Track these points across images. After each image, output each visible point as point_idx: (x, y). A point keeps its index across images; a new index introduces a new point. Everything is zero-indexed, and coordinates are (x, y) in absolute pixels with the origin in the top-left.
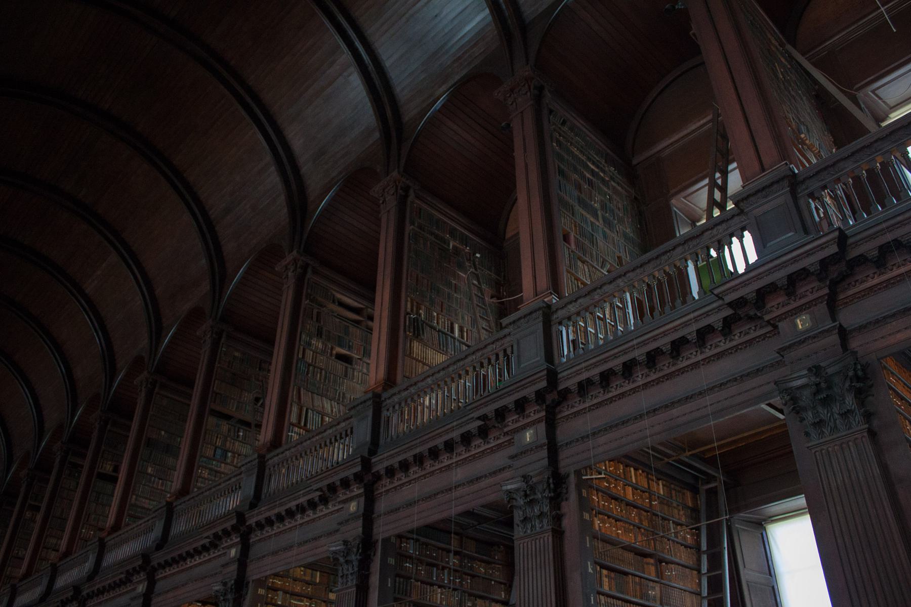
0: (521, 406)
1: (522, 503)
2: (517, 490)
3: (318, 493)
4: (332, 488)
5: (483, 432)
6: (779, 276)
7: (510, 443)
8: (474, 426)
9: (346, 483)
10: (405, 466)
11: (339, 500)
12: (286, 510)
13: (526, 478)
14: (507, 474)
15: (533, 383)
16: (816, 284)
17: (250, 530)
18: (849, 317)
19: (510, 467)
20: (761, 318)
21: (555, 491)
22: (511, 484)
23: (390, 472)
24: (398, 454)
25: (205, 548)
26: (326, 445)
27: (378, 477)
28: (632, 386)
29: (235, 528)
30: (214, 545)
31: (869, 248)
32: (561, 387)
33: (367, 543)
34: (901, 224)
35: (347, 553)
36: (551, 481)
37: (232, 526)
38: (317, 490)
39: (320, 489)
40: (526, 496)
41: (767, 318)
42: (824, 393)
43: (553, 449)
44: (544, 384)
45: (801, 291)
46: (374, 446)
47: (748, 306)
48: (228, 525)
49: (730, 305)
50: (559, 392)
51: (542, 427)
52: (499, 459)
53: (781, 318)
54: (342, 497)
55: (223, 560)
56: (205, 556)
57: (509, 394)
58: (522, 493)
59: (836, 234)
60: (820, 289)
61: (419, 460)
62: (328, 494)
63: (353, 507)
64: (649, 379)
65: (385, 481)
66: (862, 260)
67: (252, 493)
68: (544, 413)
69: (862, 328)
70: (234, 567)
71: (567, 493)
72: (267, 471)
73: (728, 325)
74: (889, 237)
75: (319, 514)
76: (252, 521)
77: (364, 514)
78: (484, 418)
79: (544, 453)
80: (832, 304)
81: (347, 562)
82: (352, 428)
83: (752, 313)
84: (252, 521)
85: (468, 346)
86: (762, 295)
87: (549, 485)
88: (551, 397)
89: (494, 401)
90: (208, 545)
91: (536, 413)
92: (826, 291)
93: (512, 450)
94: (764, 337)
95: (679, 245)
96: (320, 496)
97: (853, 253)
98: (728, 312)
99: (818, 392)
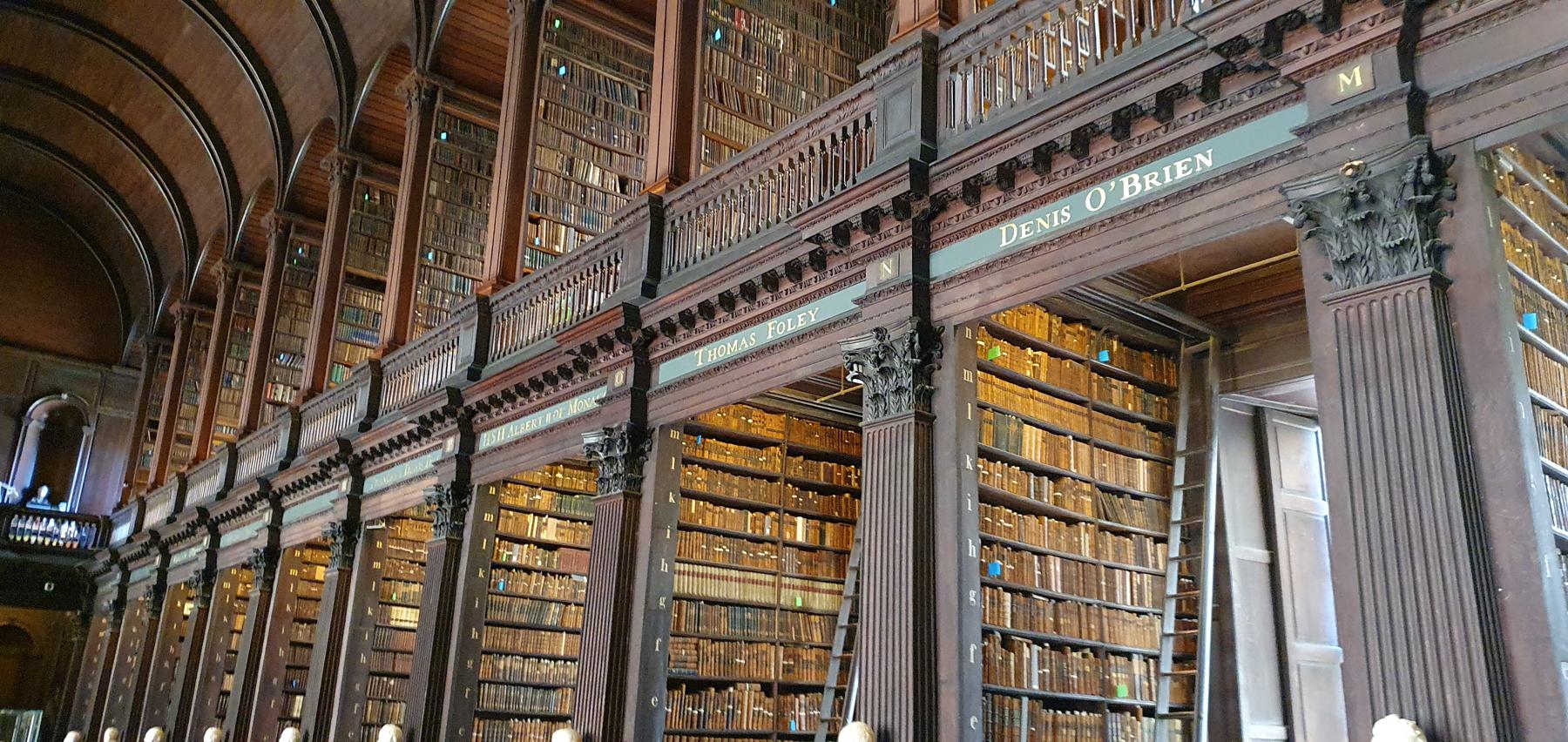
0: (872, 220)
2: (867, 351)
8: (803, 252)
13: (880, 332)
22: (859, 340)
43: (922, 288)
50: (933, 198)
51: (907, 254)
68: (910, 232)
78: (817, 239)
79: (908, 296)
91: (896, 230)
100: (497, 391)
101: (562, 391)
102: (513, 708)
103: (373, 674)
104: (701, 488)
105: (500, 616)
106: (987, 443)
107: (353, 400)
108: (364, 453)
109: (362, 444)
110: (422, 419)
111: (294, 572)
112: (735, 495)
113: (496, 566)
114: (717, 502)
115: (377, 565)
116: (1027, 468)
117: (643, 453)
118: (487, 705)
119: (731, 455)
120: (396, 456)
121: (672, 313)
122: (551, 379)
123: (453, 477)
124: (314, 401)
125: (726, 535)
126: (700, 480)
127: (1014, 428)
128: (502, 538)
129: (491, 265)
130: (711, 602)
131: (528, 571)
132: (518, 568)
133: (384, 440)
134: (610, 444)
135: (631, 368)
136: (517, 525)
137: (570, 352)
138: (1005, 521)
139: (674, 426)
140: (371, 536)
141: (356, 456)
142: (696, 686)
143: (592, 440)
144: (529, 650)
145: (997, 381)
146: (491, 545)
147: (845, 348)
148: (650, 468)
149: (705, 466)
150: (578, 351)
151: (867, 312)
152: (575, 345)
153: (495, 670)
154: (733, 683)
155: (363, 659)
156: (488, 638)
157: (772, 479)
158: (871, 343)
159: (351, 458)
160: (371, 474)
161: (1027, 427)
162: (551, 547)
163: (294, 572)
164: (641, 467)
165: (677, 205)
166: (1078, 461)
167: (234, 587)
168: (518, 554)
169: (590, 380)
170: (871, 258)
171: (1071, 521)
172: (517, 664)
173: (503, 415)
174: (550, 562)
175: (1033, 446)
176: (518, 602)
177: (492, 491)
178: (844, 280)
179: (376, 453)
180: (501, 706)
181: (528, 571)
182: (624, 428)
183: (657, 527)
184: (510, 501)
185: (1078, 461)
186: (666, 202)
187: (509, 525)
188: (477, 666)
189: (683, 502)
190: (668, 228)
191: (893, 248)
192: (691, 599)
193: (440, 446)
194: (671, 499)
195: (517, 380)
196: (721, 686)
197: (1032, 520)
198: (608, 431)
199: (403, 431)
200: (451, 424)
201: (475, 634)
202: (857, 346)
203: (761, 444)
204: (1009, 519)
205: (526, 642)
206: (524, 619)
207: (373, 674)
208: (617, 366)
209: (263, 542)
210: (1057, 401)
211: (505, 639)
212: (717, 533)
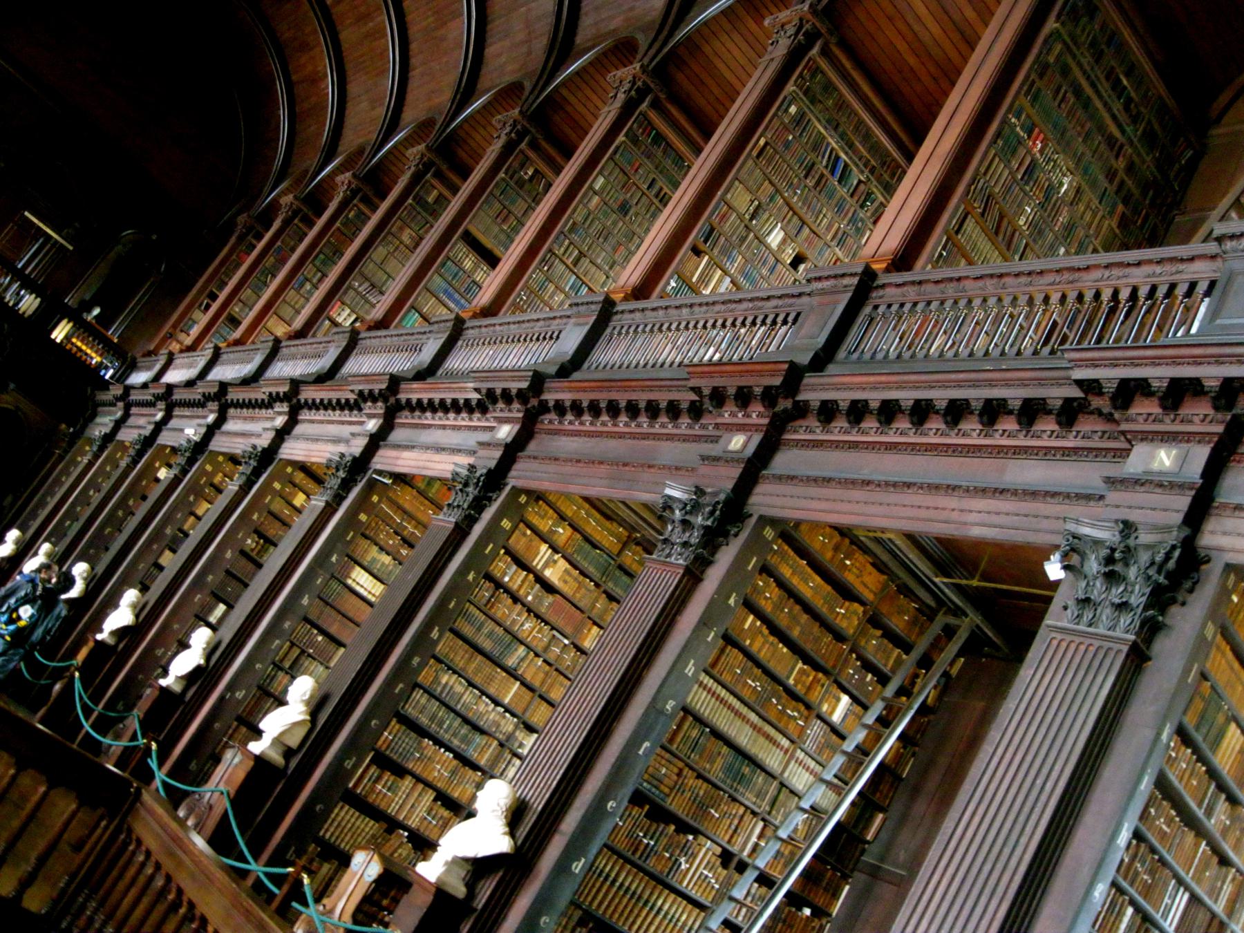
0: (1178, 393)
1: (1095, 571)
2: (1097, 543)
3: (694, 397)
4: (718, 397)
5: (1069, 414)
7: (1124, 453)
8: (1057, 394)
9: (744, 398)
10: (857, 412)
11: (719, 420)
12: (629, 402)
13: (1128, 528)
14: (1096, 509)
17: (544, 408)
19: (1102, 497)
22: (1093, 526)
23: (828, 412)
24: (887, 386)
25: (469, 407)
26: (724, 326)
27: (801, 411)
29: (522, 396)
30: (482, 407)
33: (733, 510)
35: (694, 507)
36: (1177, 553)
37: (520, 390)
38: (692, 389)
39: (696, 390)
40: (1110, 560)
46: (823, 359)
48: (515, 386)
51: (1201, 454)
52: (1088, 475)
54: (726, 417)
55: (485, 437)
56: (463, 420)
57: (1218, 360)
58: (1104, 552)
61: (921, 412)
62: (707, 404)
63: (737, 442)
65: (812, 421)
67: (571, 352)
68: (1220, 429)
70: (498, 454)
71: (1191, 591)
72: (608, 330)
75: (657, 429)
76: (550, 397)
77: (749, 461)
79: (1183, 502)
81: (686, 524)
82: (798, 314)
84: (550, 397)
87: (1168, 556)
89: (1175, 361)
90: (474, 403)
93: (1112, 470)
96: (693, 402)
100: (585, 399)
101: (657, 429)
102: (434, 728)
103: (306, 620)
104: (767, 607)
105: (467, 630)
106: (1190, 722)
107: (417, 349)
108: (409, 401)
109: (412, 391)
111: (277, 486)
112: (795, 633)
113: (489, 577)
114: (775, 630)
115: (363, 517)
116: (1212, 773)
117: (726, 535)
118: (410, 710)
119: (811, 586)
120: (438, 419)
121: (844, 397)
122: (653, 410)
123: (492, 464)
124: (379, 333)
125: (767, 672)
126: (769, 596)
128: (508, 552)
129: (632, 272)
130: (717, 734)
131: (516, 599)
132: (507, 591)
133: (437, 396)
134: (696, 507)
135: (757, 438)
136: (528, 548)
137: (696, 390)
139: (773, 522)
140: (372, 486)
141: (398, 401)
142: (659, 815)
143: (676, 494)
144: (477, 680)
145: (1230, 654)
146: (495, 554)
147: (1071, 527)
148: (726, 557)
149: (782, 584)
150: (706, 392)
151: (1113, 497)
152: (706, 385)
153: (436, 680)
154: (696, 832)
155: (305, 601)
156: (445, 644)
158: (1108, 535)
159: (392, 400)
160: (403, 425)
162: (548, 588)
163: (277, 486)
165: (890, 291)
167: (214, 474)
168: (512, 576)
169: (697, 430)
170: (1147, 437)
172: (459, 686)
173: (577, 426)
174: (541, 602)
176: (490, 625)
177: (523, 499)
178: (1090, 450)
180: (424, 720)
181: (516, 599)
182: (722, 497)
183: (705, 622)
184: (535, 520)
186: (879, 282)
187: (520, 540)
188: (423, 665)
190: (867, 310)
191: (1188, 437)
192: (699, 720)
193: (492, 429)
194: (732, 601)
195: (614, 396)
196: (684, 828)
197: (1190, 837)
198: (699, 491)
199: (461, 397)
201: (435, 634)
202: (1086, 531)
203: (846, 593)
204: (1169, 822)
205: (478, 670)
206: (487, 645)
207: (306, 620)
208: (741, 428)
209: (264, 442)
211: (460, 656)
212: (758, 664)
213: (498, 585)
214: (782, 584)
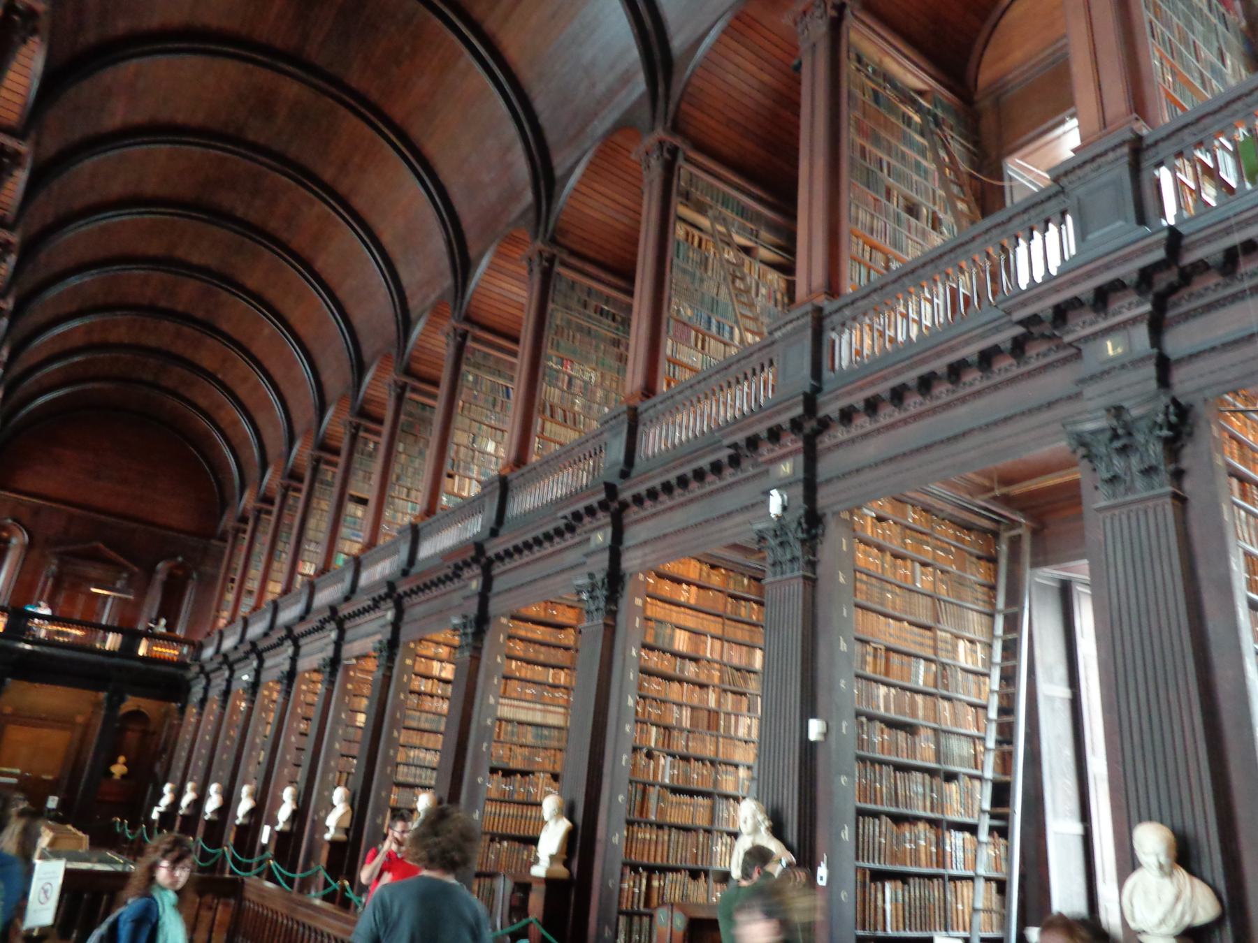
6: (1084, 289)
15: (788, 409)
16: (1134, 298)
18: (1178, 341)
20: (1060, 338)
21: (808, 531)
28: (904, 415)
31: (1212, 251)
32: (821, 414)
34: (1247, 223)
41: (1068, 339)
42: (1122, 435)
44: (799, 410)
45: (1113, 307)
47: (1048, 325)
49: (1021, 323)
53: (1086, 339)
59: (1165, 234)
60: (1138, 304)
64: (923, 408)
66: (1202, 267)
69: (1193, 357)
73: (1019, 347)
74: (1237, 238)
80: (1157, 326)
83: (1047, 333)
85: (561, 444)
86: (1061, 313)
88: (809, 426)
92: (1147, 307)
94: (1065, 361)
95: (847, 305)
97: (1189, 258)
98: (1019, 330)
99: (1115, 436)
102: (417, 781)
103: (343, 756)
105: (414, 724)
107: (343, 580)
110: (374, 599)
111: (304, 687)
112: (542, 658)
113: (412, 692)
115: (350, 686)
116: (675, 655)
118: (400, 778)
119: (539, 633)
125: (535, 683)
126: (518, 648)
127: (668, 631)
128: (416, 675)
130: (521, 723)
131: (432, 696)
132: (425, 694)
135: (480, 579)
136: (427, 667)
138: (654, 686)
140: (347, 668)
142: (508, 773)
144: (430, 746)
145: (660, 604)
146: (410, 679)
149: (522, 640)
153: (408, 756)
154: (533, 773)
155: (337, 746)
156: (403, 737)
157: (567, 649)
161: (678, 631)
163: (304, 687)
164: (482, 640)
166: (710, 649)
167: (271, 694)
168: (424, 686)
171: (703, 686)
172: (422, 754)
175: (681, 642)
176: (424, 716)
179: (352, 616)
180: (411, 780)
181: (432, 696)
184: (425, 652)
185: (710, 649)
187: (421, 666)
188: (396, 754)
189: (506, 662)
192: (509, 721)
194: (499, 660)
196: (525, 773)
197: (676, 685)
200: (390, 603)
201: (396, 734)
204: (659, 684)
205: (428, 740)
206: (426, 726)
207: (343, 756)
209: (286, 667)
210: (701, 615)
211: (415, 738)
212: (529, 681)
213: (420, 694)
214: (522, 640)
